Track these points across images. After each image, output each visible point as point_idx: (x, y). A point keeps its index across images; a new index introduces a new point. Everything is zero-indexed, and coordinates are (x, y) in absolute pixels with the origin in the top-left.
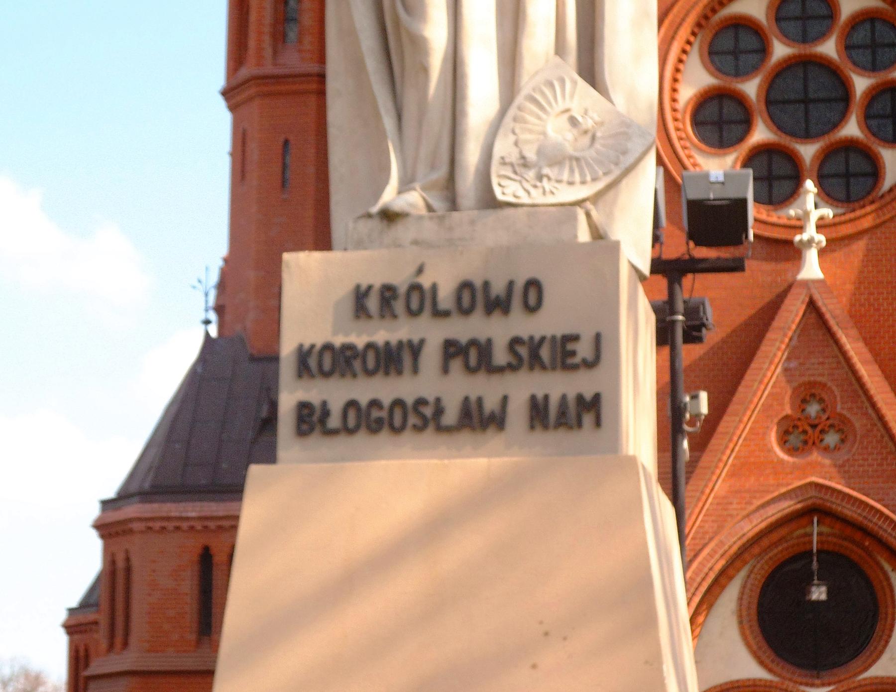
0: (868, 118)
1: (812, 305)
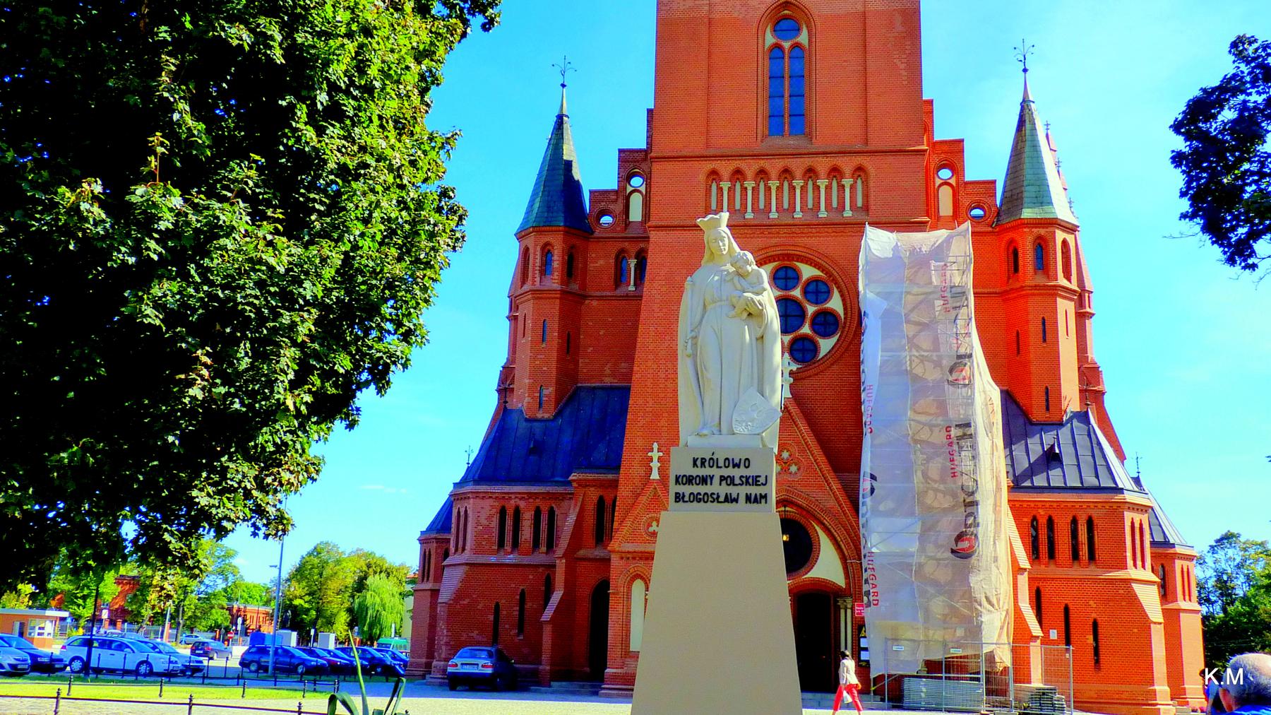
0: (813, 326)
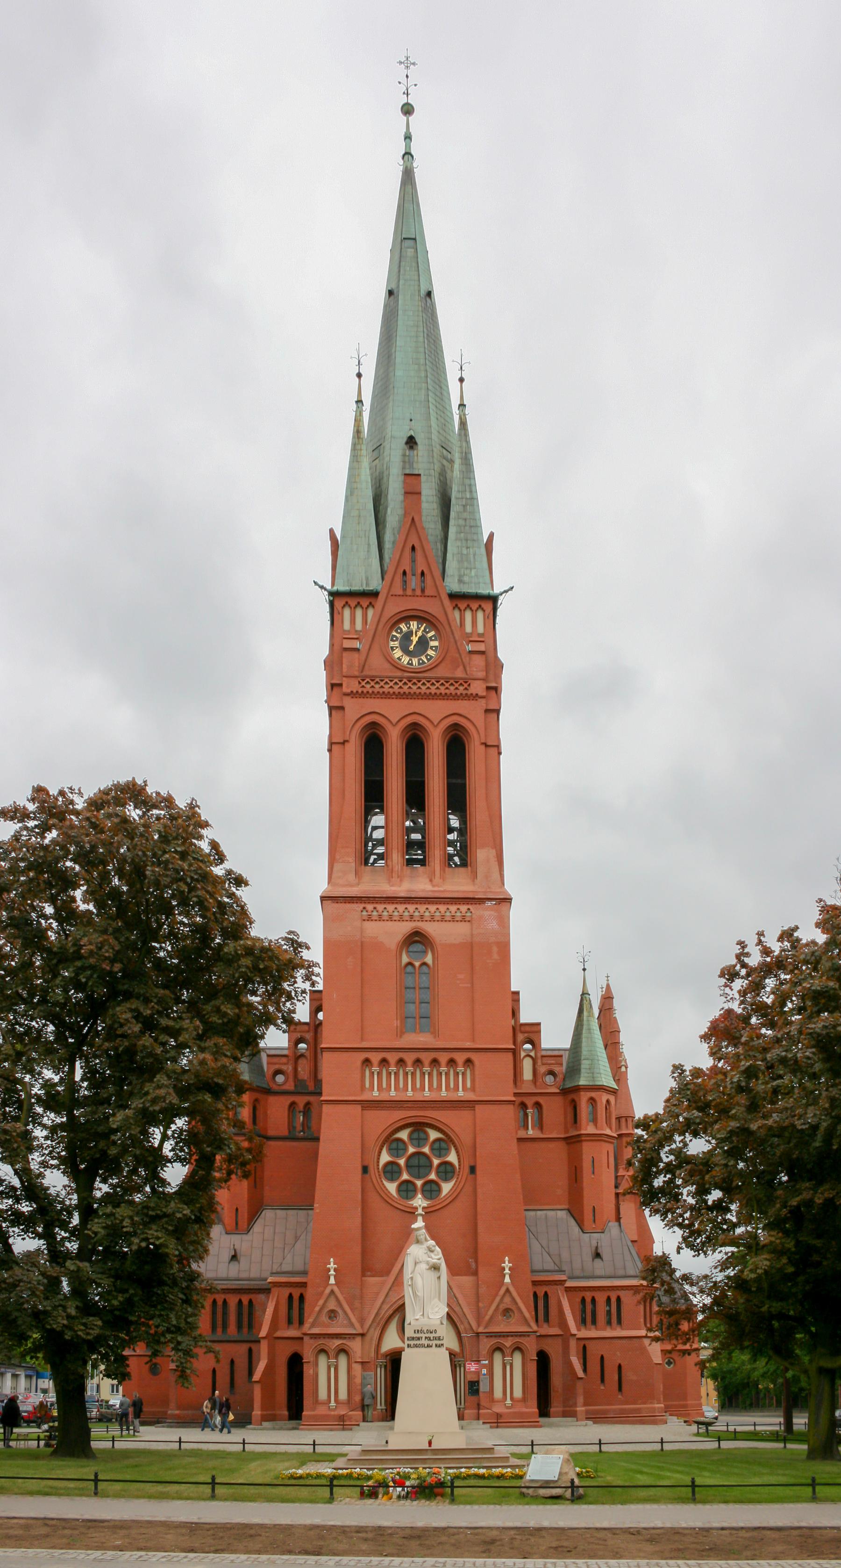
0: (437, 1173)
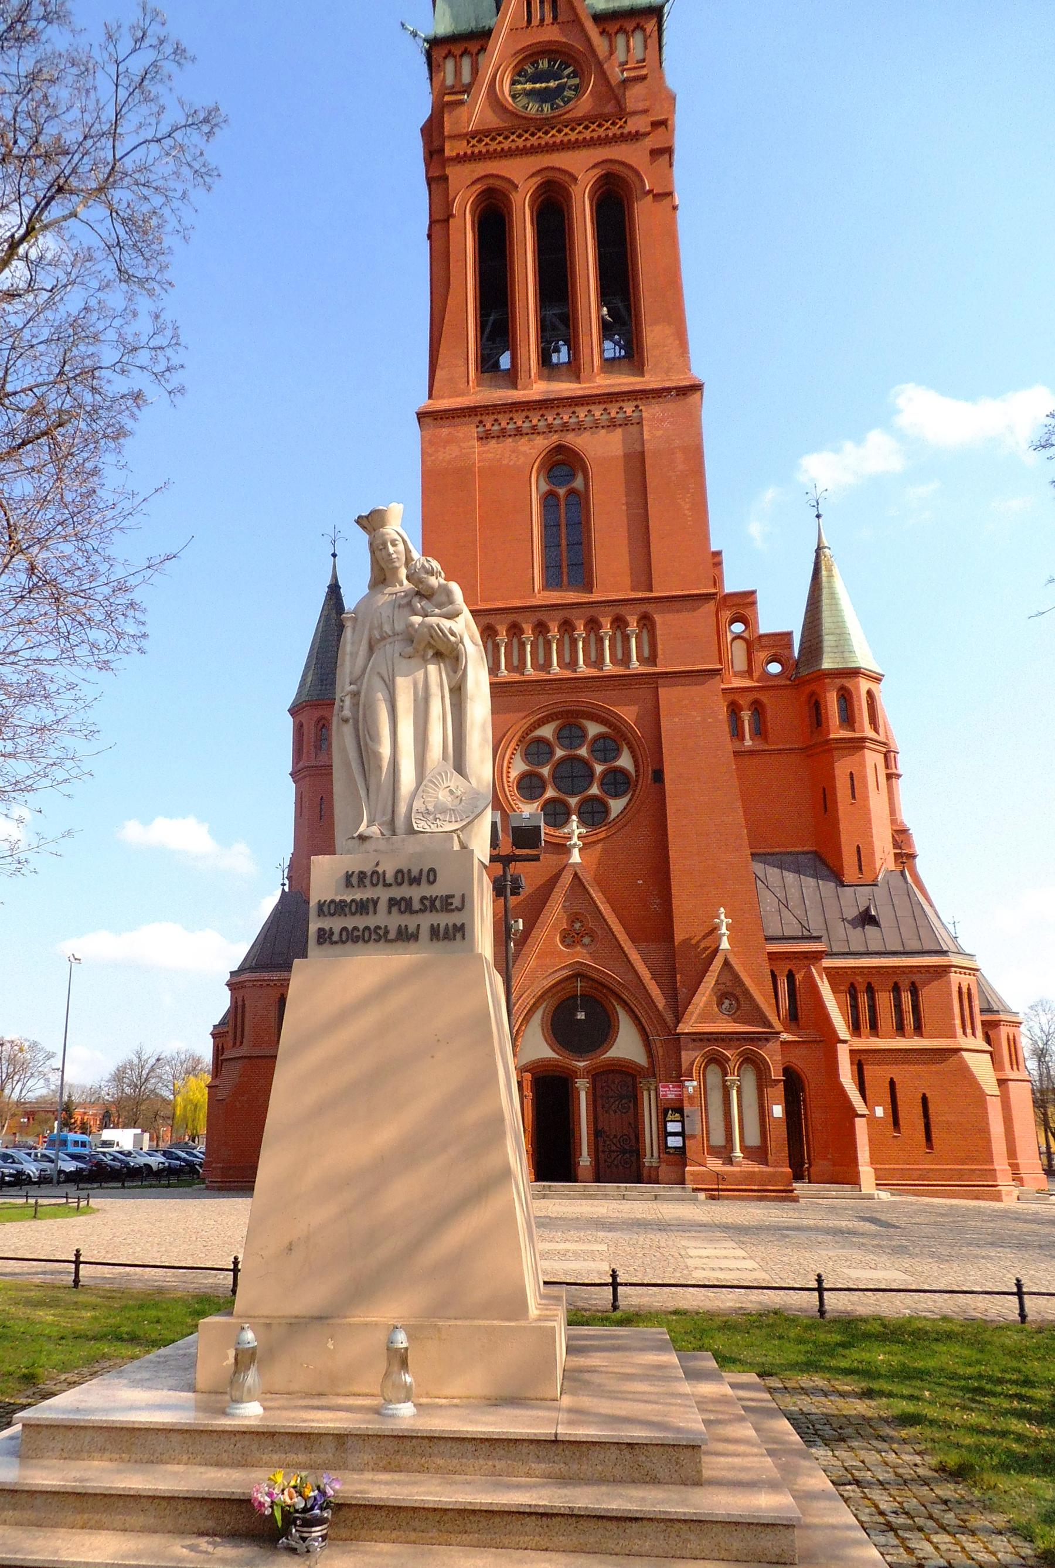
0: (602, 785)
1: (576, 874)
